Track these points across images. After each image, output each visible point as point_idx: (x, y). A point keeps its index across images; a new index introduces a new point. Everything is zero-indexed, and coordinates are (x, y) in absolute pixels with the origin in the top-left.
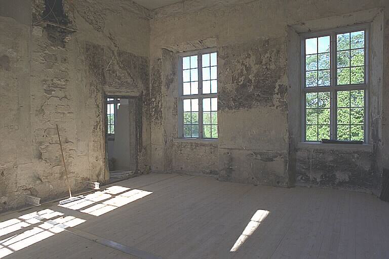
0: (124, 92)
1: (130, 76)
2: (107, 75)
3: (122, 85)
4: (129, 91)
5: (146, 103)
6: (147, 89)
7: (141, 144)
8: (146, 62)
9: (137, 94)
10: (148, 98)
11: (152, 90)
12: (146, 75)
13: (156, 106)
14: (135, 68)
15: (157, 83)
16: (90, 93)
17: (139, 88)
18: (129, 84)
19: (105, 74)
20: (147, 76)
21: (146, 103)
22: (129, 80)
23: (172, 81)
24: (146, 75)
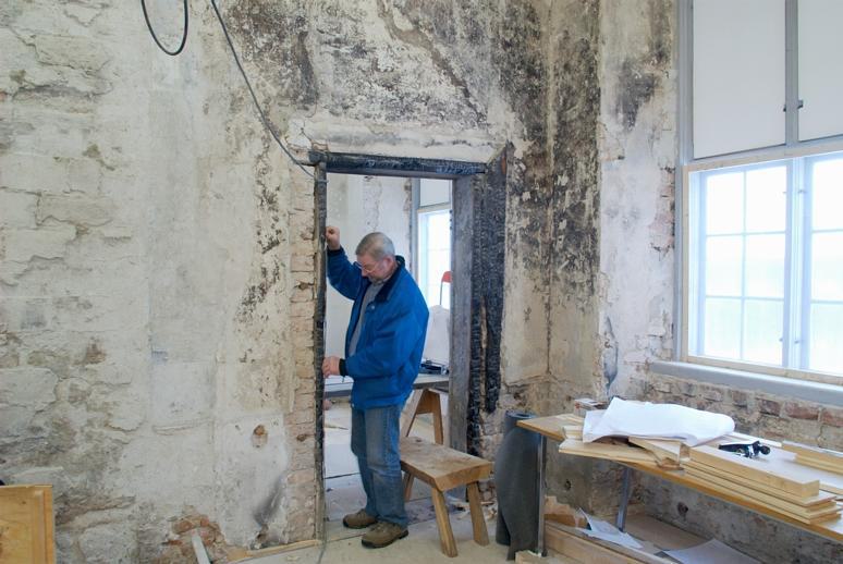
0: (416, 142)
1: (449, 72)
2: (324, 63)
3: (402, 108)
4: (438, 138)
5: (526, 196)
6: (536, 132)
7: (493, 377)
8: (532, 16)
9: (485, 156)
10: (540, 174)
11: (557, 137)
12: (531, 73)
13: (573, 208)
14: (474, 37)
15: (580, 104)
16: (228, 142)
17: (493, 131)
18: (438, 107)
19: (315, 59)
20: (538, 77)
21: (526, 196)
22: (445, 91)
23: (649, 88)
24: (531, 73)
